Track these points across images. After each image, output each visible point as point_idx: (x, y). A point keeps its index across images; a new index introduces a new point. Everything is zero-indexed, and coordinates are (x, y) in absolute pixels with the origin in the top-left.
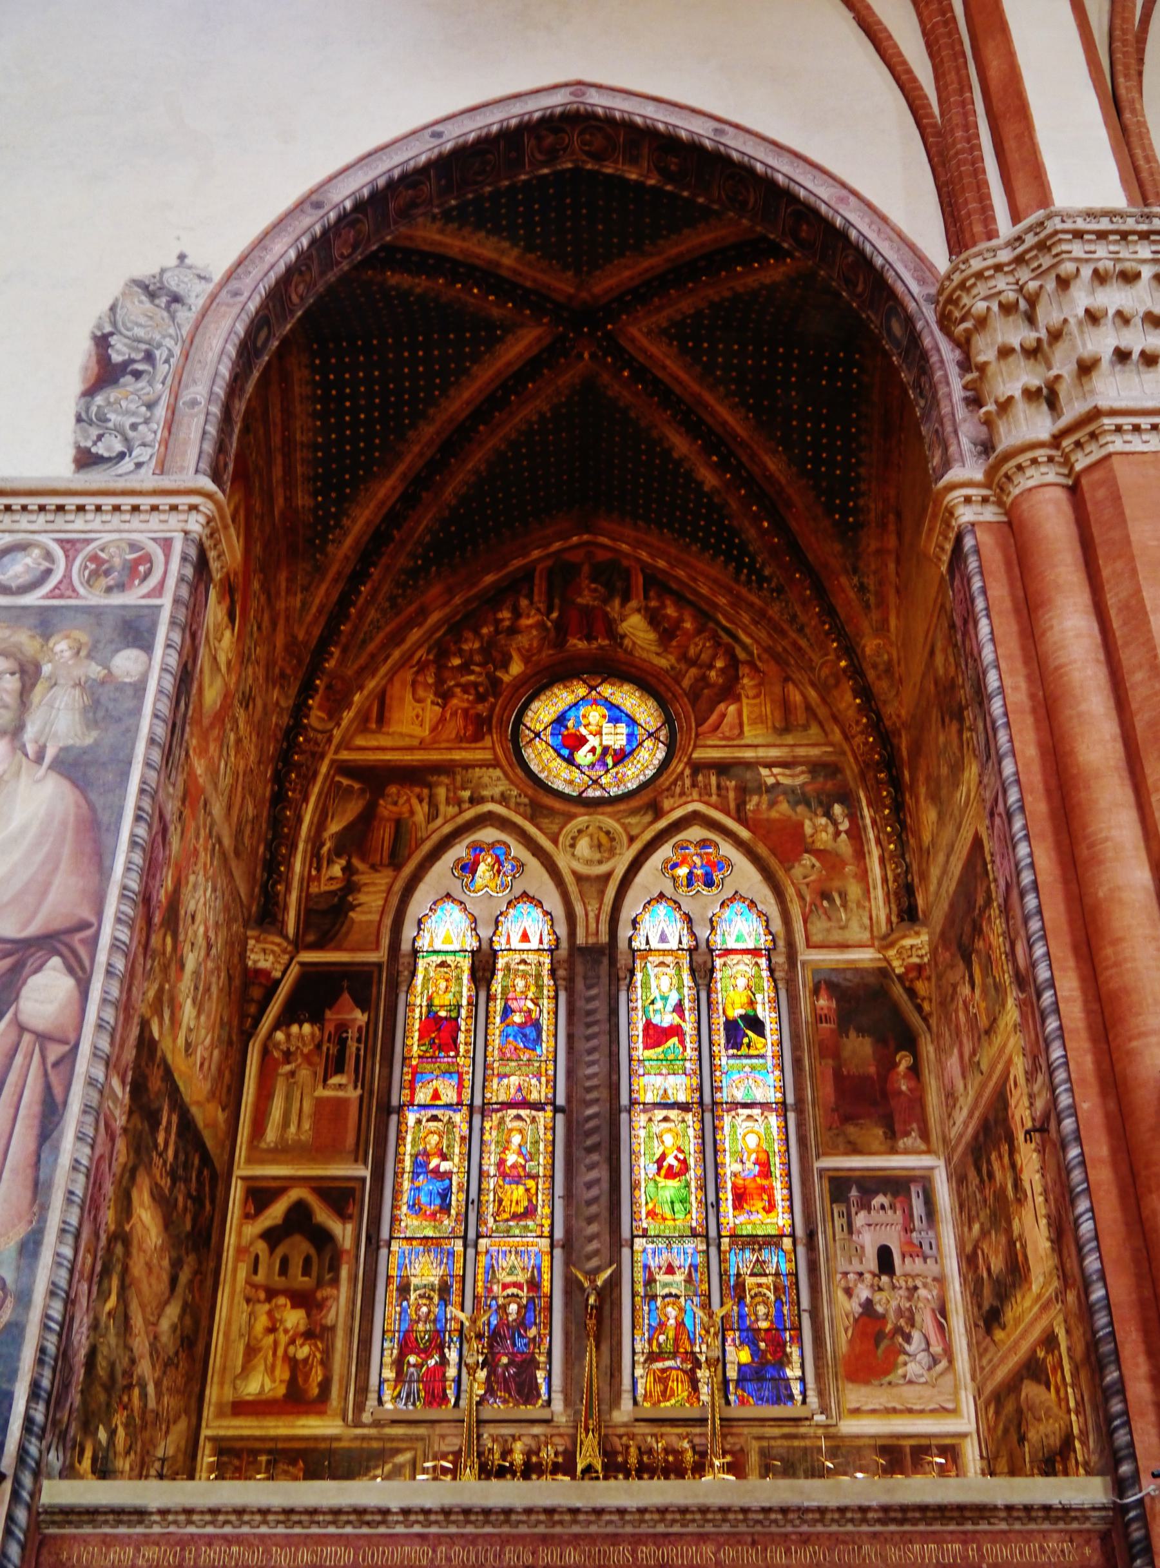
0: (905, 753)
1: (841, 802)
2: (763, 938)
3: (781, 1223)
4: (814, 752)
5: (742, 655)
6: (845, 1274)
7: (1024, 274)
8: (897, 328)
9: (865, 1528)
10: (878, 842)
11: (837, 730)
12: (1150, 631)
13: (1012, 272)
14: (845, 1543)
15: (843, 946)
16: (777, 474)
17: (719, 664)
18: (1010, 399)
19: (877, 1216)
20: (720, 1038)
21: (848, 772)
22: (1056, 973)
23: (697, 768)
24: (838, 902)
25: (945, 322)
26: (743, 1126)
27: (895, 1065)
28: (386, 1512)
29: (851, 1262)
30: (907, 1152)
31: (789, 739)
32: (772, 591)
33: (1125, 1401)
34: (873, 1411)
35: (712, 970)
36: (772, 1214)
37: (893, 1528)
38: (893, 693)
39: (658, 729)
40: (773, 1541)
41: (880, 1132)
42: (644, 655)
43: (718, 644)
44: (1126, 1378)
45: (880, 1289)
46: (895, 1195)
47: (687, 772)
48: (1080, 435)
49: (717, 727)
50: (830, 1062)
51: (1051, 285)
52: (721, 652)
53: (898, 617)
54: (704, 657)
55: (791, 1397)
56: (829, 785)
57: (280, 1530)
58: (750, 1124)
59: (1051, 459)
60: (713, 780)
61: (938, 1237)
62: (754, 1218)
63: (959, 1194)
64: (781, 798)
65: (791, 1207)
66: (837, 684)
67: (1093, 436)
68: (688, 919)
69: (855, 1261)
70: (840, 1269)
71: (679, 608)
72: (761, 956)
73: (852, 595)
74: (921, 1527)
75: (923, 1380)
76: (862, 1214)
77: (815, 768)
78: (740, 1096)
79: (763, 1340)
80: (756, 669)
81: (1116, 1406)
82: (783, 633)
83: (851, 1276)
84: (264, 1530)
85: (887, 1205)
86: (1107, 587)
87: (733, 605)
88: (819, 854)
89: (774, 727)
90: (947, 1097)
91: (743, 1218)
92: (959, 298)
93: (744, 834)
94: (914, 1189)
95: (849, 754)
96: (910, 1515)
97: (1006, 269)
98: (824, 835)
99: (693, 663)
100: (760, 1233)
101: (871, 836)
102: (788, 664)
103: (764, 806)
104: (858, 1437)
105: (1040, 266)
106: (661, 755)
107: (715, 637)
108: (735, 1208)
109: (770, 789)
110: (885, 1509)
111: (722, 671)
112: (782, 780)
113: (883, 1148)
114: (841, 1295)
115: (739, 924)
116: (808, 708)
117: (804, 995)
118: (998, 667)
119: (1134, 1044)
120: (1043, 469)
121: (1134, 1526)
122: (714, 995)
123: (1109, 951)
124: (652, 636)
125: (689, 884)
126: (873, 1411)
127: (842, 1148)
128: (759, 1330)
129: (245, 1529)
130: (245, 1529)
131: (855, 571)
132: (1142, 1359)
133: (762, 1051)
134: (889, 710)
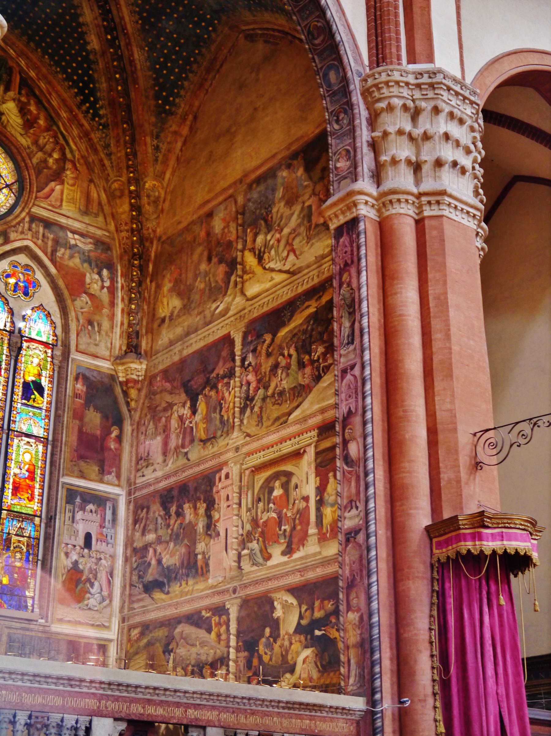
0: (153, 255)
1: (108, 269)
2: (52, 337)
3: (36, 508)
4: (99, 233)
5: (69, 156)
6: (67, 544)
7: (417, 94)
8: (332, 76)
9: (276, 710)
10: (123, 300)
11: (113, 224)
12: (448, 316)
13: (412, 89)
14: (268, 716)
15: (95, 356)
16: (137, 62)
17: (56, 155)
18: (401, 160)
19: (88, 516)
20: (19, 391)
21: (114, 252)
22: (376, 466)
23: (34, 218)
24: (96, 329)
25: (366, 93)
26: (24, 447)
27: (110, 433)
28: (82, 681)
29: (70, 539)
30: (108, 483)
31: (87, 219)
32: (100, 124)
33: (381, 667)
34: (69, 622)
35: (20, 348)
36: (32, 503)
37: (286, 711)
38: (155, 216)
39: (12, 184)
40: (241, 713)
41: (96, 469)
42: (13, 132)
43: (57, 143)
44: (382, 658)
45: (83, 556)
46: (99, 506)
47: (27, 219)
48: (433, 199)
49: (47, 197)
50: (78, 422)
51: (429, 108)
52: (58, 148)
53: (173, 174)
54: (48, 148)
55: (26, 607)
56: (103, 256)
57: (28, 684)
58: (28, 447)
59: (414, 203)
60: (41, 229)
61: (115, 534)
62: (23, 503)
63: (135, 513)
64: (76, 255)
65: (42, 500)
66: (121, 196)
67: (438, 203)
68: (11, 312)
69: (73, 538)
70: (65, 542)
71: (38, 109)
72: (49, 348)
73: (150, 150)
74: (296, 712)
75: (96, 609)
76: (81, 513)
77: (98, 242)
78: (25, 429)
79: (17, 573)
80: (76, 169)
81: (377, 669)
82: (96, 151)
83: (69, 546)
84: (20, 683)
85: (93, 511)
86: (429, 283)
87: (69, 120)
88: (92, 296)
89: (80, 209)
90: (139, 460)
91: (16, 501)
92: (382, 88)
93: (53, 270)
94: (109, 504)
95: (117, 241)
96: (295, 706)
97: (410, 87)
98: (95, 285)
99: (41, 149)
100: (24, 511)
101: (120, 294)
102: (93, 171)
103: (66, 257)
104: (59, 634)
105: (427, 95)
106: (11, 201)
107: (55, 137)
108: (13, 495)
109: (71, 247)
110: (287, 703)
111: (56, 160)
112: (79, 244)
113: (97, 478)
114: (63, 555)
115: (39, 324)
116: (100, 204)
117: (70, 378)
118: (368, 300)
119: (412, 511)
120: (409, 207)
121: (379, 720)
122: (19, 364)
123: (407, 465)
124: (19, 121)
125: (15, 291)
126: (69, 622)
127: (76, 473)
128: (15, 567)
129: (10, 682)
130: (10, 682)
131: (157, 137)
132: (388, 650)
133: (41, 406)
134: (150, 225)
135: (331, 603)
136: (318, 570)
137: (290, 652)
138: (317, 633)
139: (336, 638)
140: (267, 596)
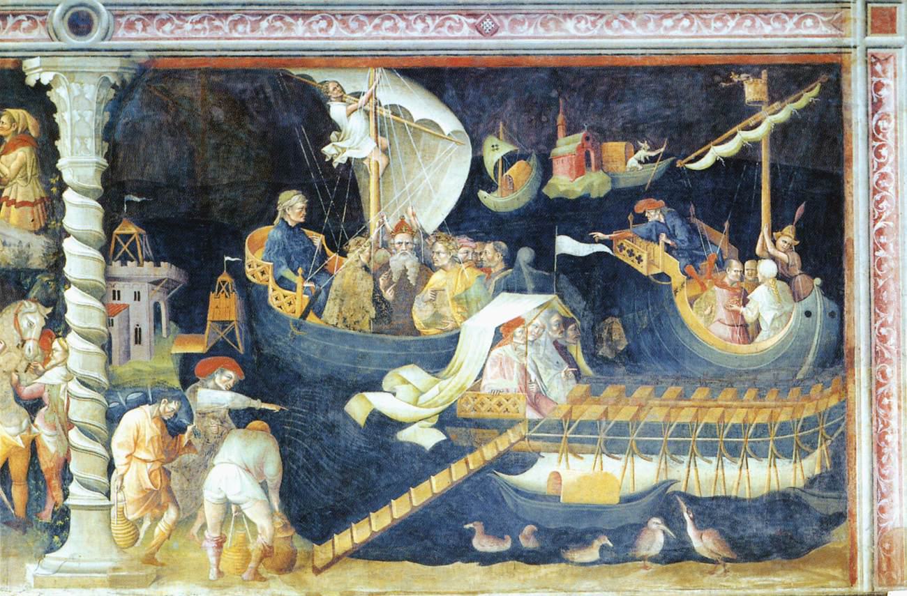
135: (642, 154)
136: (570, 25)
137: (427, 293)
138: (566, 245)
139: (663, 276)
140: (288, 77)
